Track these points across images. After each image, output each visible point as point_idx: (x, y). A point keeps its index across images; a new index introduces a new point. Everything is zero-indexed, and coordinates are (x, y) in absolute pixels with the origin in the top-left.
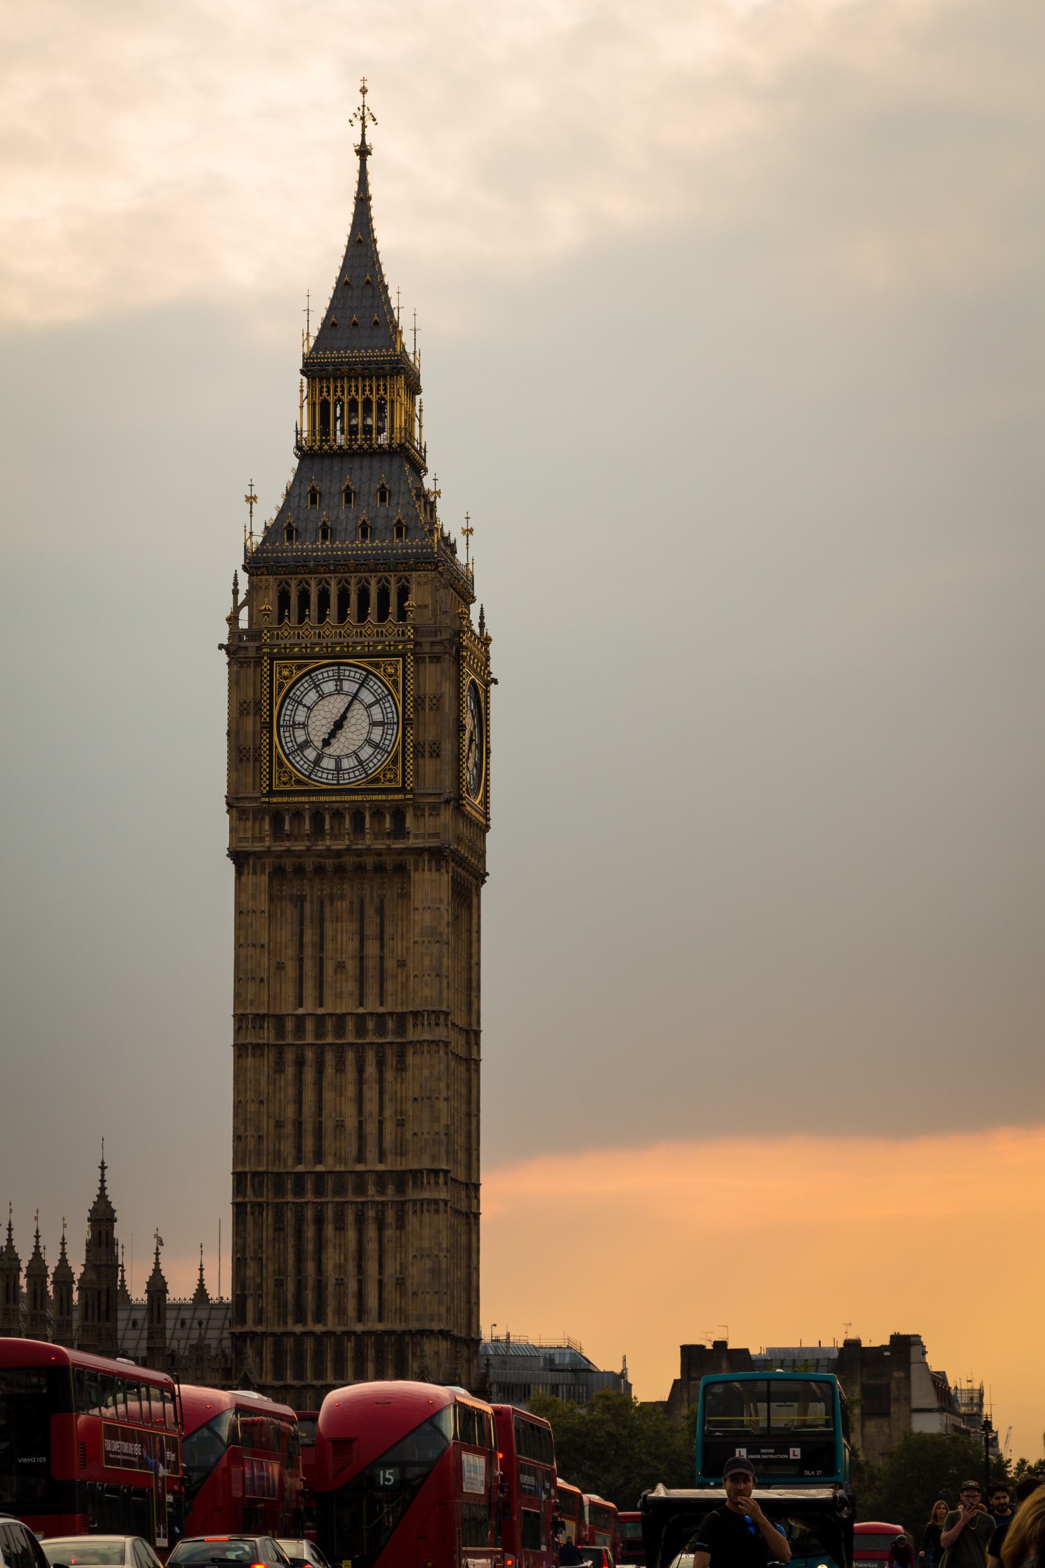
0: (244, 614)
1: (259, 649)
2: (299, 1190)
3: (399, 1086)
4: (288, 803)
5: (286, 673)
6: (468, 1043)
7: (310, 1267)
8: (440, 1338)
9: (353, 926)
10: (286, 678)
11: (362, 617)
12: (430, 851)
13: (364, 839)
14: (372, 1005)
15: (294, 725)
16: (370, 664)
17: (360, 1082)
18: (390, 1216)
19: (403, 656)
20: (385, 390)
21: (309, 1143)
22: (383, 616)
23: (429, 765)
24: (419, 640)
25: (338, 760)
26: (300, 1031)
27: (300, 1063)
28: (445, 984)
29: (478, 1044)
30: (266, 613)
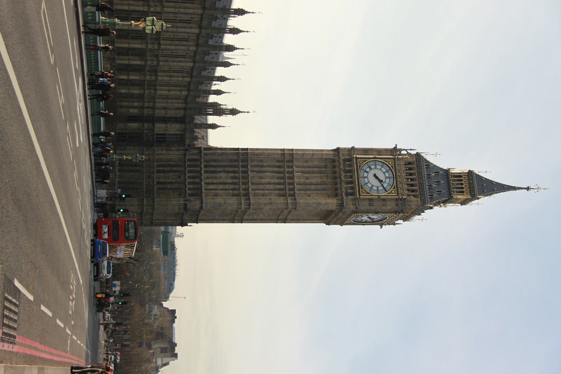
2: (243, 166)
3: (274, 195)
4: (354, 163)
5: (390, 163)
6: (283, 219)
7: (221, 169)
8: (200, 206)
10: (389, 163)
12: (343, 203)
13: (345, 185)
15: (376, 165)
16: (395, 186)
17: (275, 184)
18: (236, 192)
19: (398, 195)
20: (467, 193)
21: (257, 169)
23: (367, 203)
25: (367, 177)
26: (289, 167)
27: (279, 167)
28: (304, 208)
29: (282, 222)
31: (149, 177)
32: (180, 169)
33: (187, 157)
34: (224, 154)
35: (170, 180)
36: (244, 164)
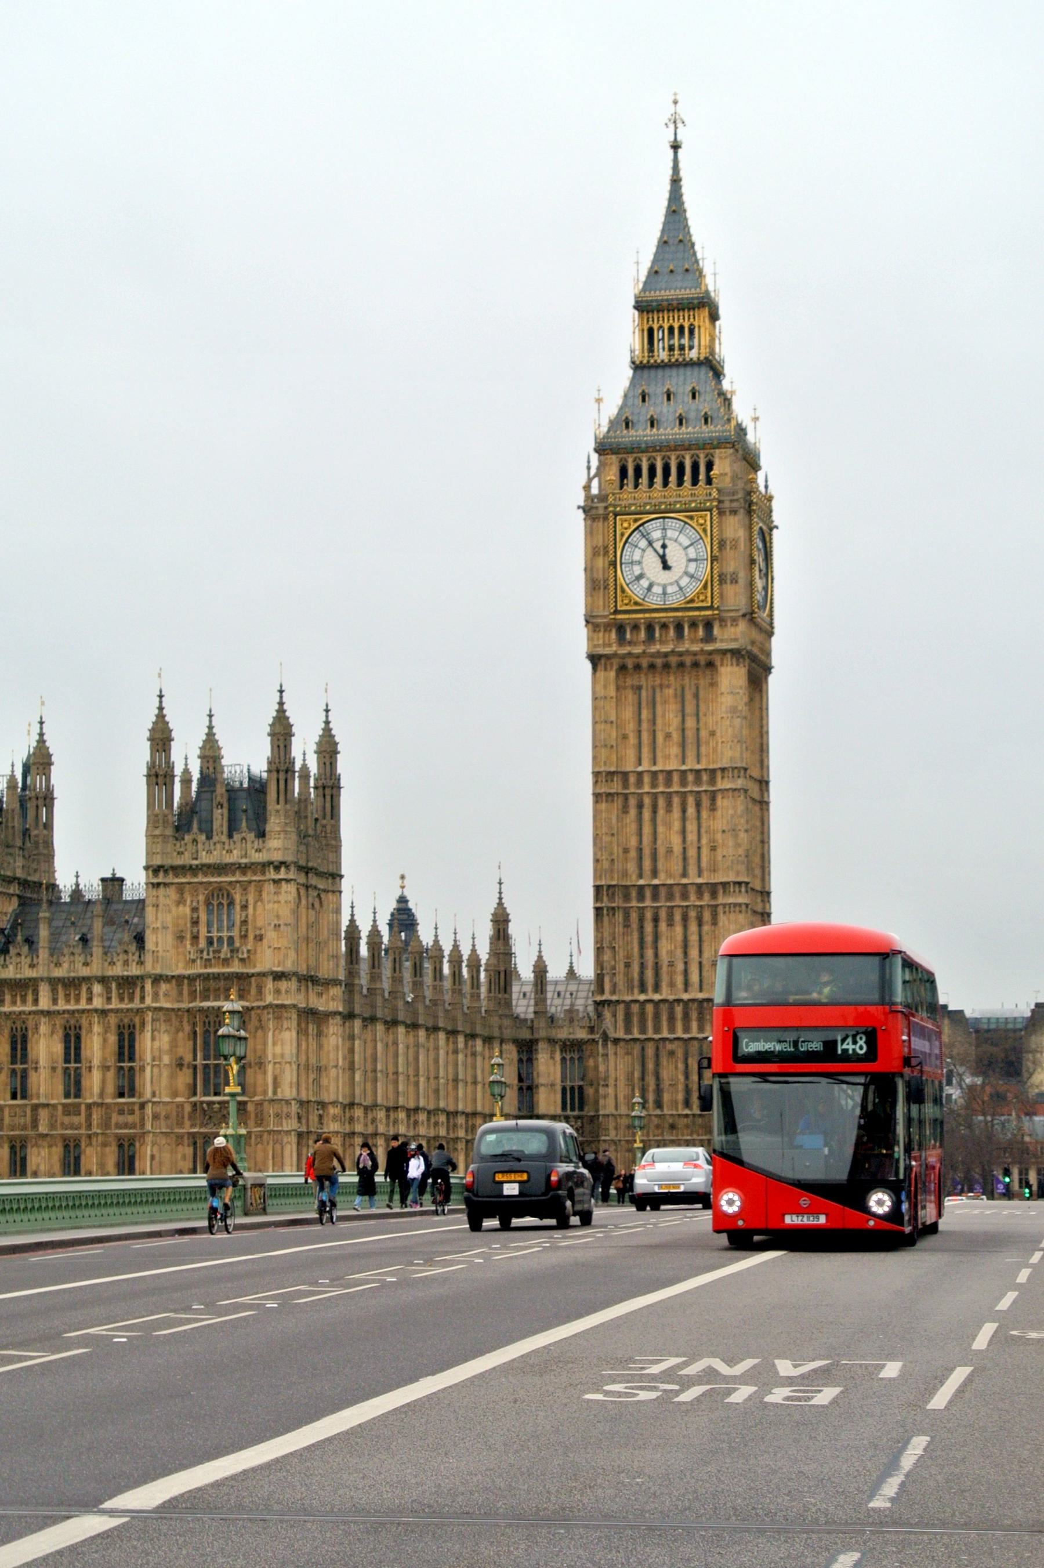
0: (595, 483)
1: (606, 508)
2: (641, 897)
5: (626, 525)
7: (649, 953)
9: (679, 706)
11: (680, 482)
14: (691, 764)
16: (687, 517)
17: (684, 819)
18: (707, 916)
21: (647, 864)
22: (695, 481)
23: (730, 590)
24: (722, 498)
25: (664, 587)
26: (639, 783)
27: (640, 806)
29: (768, 790)
30: (611, 482)
31: (673, 1127)
32: (650, 1051)
33: (621, 1034)
34: (610, 943)
35: (681, 1078)
36: (634, 894)
